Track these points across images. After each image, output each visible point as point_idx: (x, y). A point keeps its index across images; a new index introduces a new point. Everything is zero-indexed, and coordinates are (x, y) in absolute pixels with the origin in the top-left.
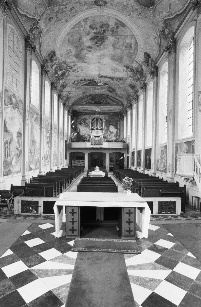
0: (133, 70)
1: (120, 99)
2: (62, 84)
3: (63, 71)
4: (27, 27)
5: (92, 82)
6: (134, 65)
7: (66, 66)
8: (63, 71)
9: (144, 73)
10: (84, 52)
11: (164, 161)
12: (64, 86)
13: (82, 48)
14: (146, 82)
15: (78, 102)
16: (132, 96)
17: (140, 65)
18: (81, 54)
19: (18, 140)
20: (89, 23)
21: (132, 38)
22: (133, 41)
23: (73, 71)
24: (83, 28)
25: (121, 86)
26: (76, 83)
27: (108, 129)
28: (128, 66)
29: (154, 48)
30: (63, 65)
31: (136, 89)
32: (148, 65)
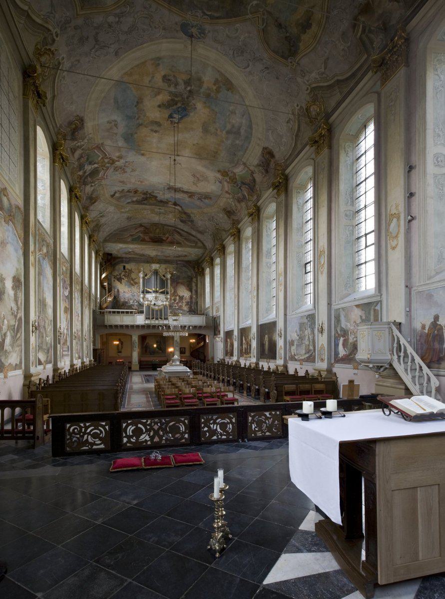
0: (235, 180)
1: (199, 236)
2: (90, 193)
3: (96, 166)
4: (30, 42)
5: (147, 198)
6: (239, 171)
7: (101, 156)
8: (96, 166)
9: (257, 186)
10: (144, 131)
12: (92, 200)
13: (141, 123)
14: (259, 204)
15: (117, 236)
16: (225, 231)
17: (250, 172)
18: (136, 136)
19: (15, 294)
21: (243, 116)
22: (244, 121)
23: (116, 169)
25: (205, 211)
26: (119, 197)
27: (175, 294)
29: (284, 140)
31: (236, 218)
32: (267, 171)
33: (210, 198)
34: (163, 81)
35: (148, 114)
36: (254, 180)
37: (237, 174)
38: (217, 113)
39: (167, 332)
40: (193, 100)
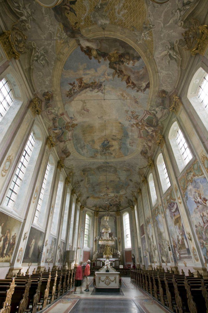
0: (66, 128)
3: (146, 128)
8: (146, 128)
10: (119, 137)
11: (52, 252)
13: (120, 140)
18: (123, 135)
20: (113, 156)
21: (84, 154)
22: (82, 152)
24: (117, 154)
28: (74, 129)
30: (142, 134)
33: (67, 97)
34: (112, 153)
35: (117, 143)
36: (61, 142)
37: (68, 132)
38: (92, 149)
39: (74, 144)
40: (101, 150)
